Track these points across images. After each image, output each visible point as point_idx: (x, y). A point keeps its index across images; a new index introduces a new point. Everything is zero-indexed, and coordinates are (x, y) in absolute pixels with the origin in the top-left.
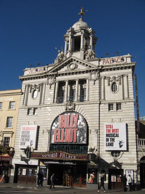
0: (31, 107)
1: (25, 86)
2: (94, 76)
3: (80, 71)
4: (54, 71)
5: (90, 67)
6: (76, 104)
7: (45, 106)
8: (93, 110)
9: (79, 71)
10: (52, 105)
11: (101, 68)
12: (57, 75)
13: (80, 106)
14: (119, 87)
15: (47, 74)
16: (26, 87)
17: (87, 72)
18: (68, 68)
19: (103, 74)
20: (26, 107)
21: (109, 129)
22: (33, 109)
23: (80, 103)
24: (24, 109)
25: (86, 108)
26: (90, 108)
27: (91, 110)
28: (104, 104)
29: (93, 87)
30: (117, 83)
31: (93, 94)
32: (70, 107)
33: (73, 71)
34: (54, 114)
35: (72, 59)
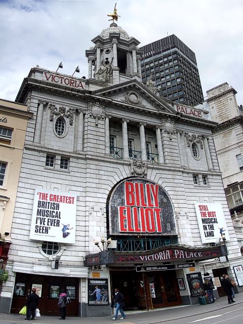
0: (57, 152)
1: (37, 102)
2: (169, 125)
3: (145, 109)
4: (104, 94)
5: (164, 109)
6: (149, 166)
7: (90, 157)
8: (176, 181)
9: (143, 109)
10: (105, 159)
11: (179, 116)
12: (109, 105)
13: (155, 172)
14: (201, 152)
15: (92, 96)
16: (39, 104)
17: (160, 117)
18: (126, 98)
19: (181, 127)
20: (43, 149)
21: (204, 211)
22: (59, 157)
23: (155, 166)
24: (36, 153)
25: (164, 176)
26: (170, 176)
27: (172, 180)
28: (188, 173)
29: (171, 143)
30: (199, 145)
31: (171, 154)
32: (139, 171)
33: (134, 107)
34: (110, 178)
35: (134, 85)
